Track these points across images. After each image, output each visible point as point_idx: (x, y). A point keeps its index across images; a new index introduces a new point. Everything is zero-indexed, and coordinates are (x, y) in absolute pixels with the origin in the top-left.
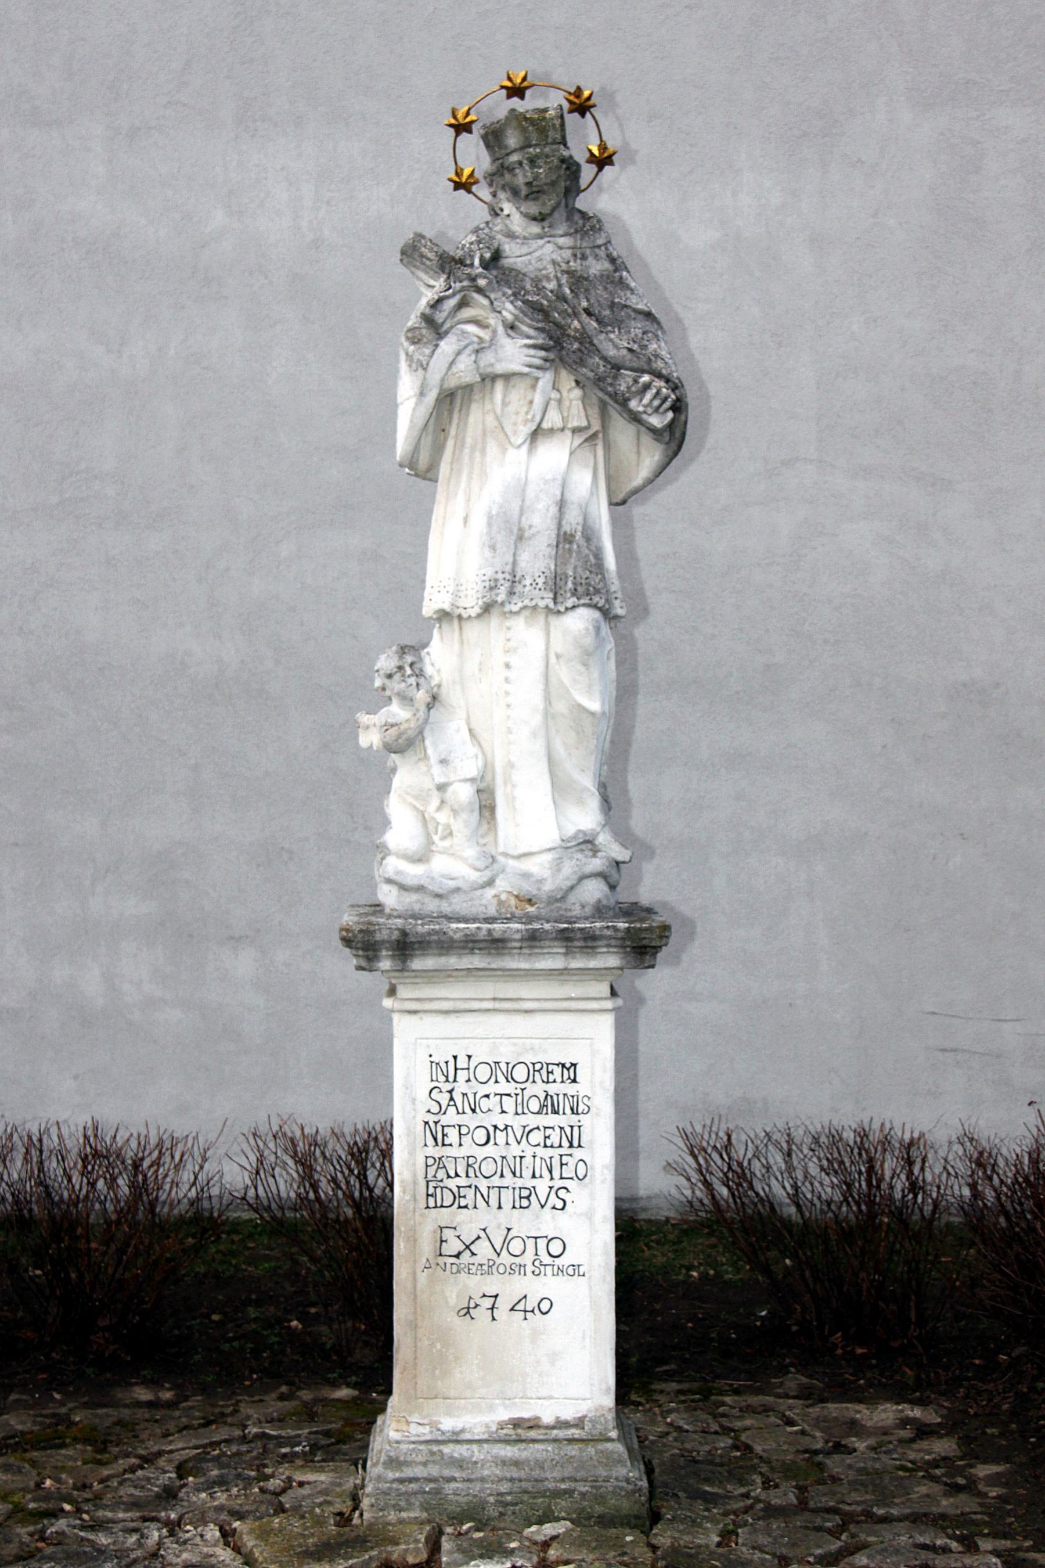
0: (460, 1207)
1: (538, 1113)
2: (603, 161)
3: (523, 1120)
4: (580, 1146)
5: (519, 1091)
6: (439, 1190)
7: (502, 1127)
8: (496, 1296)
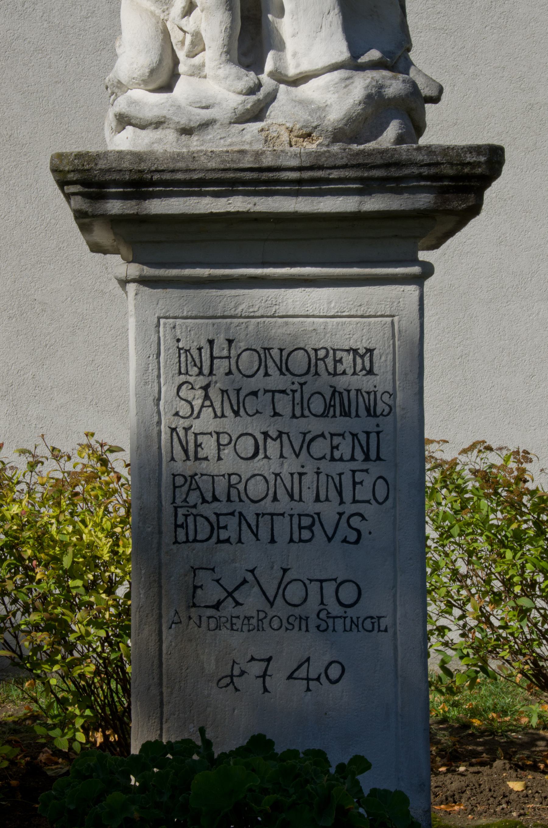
0: (219, 541)
1: (322, 416)
3: (303, 424)
4: (378, 458)
5: (296, 387)
6: (190, 519)
7: (274, 434)
8: (269, 660)
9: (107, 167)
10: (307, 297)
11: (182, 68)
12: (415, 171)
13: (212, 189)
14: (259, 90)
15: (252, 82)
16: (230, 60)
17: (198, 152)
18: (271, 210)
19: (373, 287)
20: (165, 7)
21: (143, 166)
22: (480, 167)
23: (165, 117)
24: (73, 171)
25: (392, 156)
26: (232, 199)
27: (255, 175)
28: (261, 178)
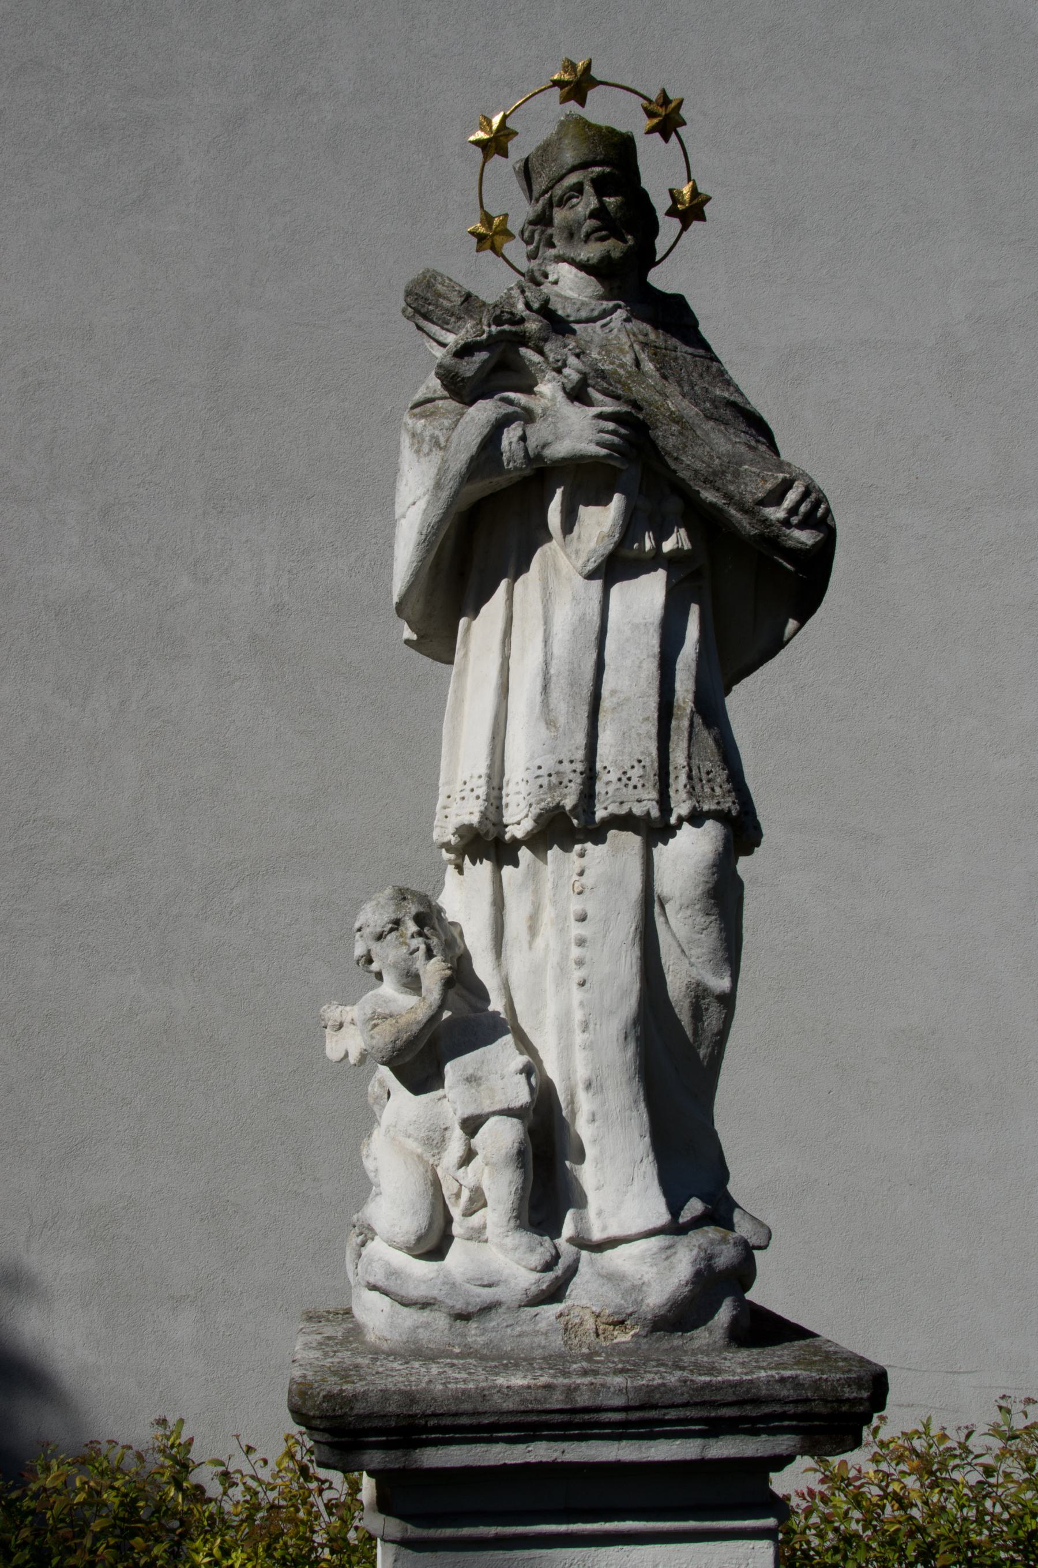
2: (691, 212)
9: (367, 1411)
10: (625, 1558)
11: (456, 1229)
12: (778, 1409)
13: (506, 1434)
14: (556, 1263)
15: (548, 1254)
16: (520, 1227)
17: (490, 1388)
18: (586, 1460)
19: (713, 1543)
20: (436, 1151)
21: (416, 1409)
22: (861, 1404)
23: (435, 1299)
24: (321, 1418)
25: (748, 1391)
26: (532, 1446)
27: (565, 1418)
28: (577, 1422)
